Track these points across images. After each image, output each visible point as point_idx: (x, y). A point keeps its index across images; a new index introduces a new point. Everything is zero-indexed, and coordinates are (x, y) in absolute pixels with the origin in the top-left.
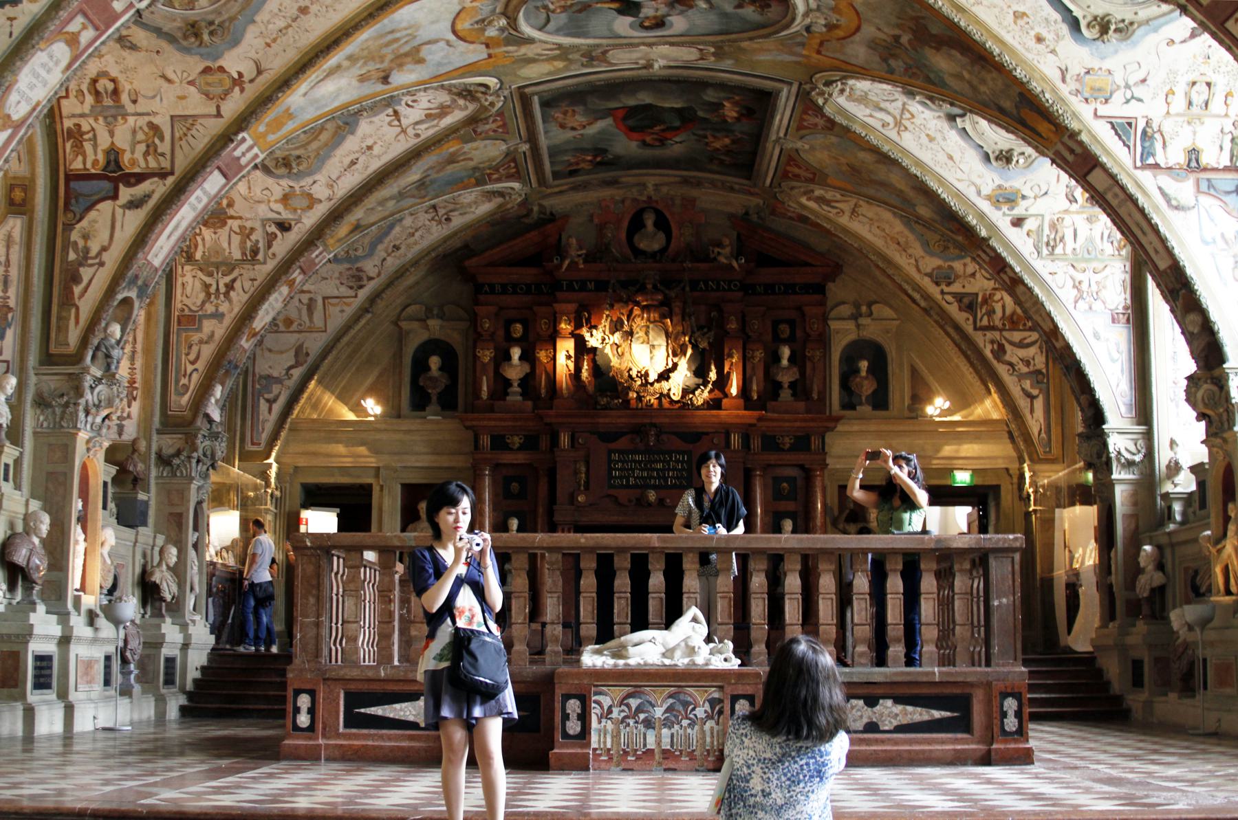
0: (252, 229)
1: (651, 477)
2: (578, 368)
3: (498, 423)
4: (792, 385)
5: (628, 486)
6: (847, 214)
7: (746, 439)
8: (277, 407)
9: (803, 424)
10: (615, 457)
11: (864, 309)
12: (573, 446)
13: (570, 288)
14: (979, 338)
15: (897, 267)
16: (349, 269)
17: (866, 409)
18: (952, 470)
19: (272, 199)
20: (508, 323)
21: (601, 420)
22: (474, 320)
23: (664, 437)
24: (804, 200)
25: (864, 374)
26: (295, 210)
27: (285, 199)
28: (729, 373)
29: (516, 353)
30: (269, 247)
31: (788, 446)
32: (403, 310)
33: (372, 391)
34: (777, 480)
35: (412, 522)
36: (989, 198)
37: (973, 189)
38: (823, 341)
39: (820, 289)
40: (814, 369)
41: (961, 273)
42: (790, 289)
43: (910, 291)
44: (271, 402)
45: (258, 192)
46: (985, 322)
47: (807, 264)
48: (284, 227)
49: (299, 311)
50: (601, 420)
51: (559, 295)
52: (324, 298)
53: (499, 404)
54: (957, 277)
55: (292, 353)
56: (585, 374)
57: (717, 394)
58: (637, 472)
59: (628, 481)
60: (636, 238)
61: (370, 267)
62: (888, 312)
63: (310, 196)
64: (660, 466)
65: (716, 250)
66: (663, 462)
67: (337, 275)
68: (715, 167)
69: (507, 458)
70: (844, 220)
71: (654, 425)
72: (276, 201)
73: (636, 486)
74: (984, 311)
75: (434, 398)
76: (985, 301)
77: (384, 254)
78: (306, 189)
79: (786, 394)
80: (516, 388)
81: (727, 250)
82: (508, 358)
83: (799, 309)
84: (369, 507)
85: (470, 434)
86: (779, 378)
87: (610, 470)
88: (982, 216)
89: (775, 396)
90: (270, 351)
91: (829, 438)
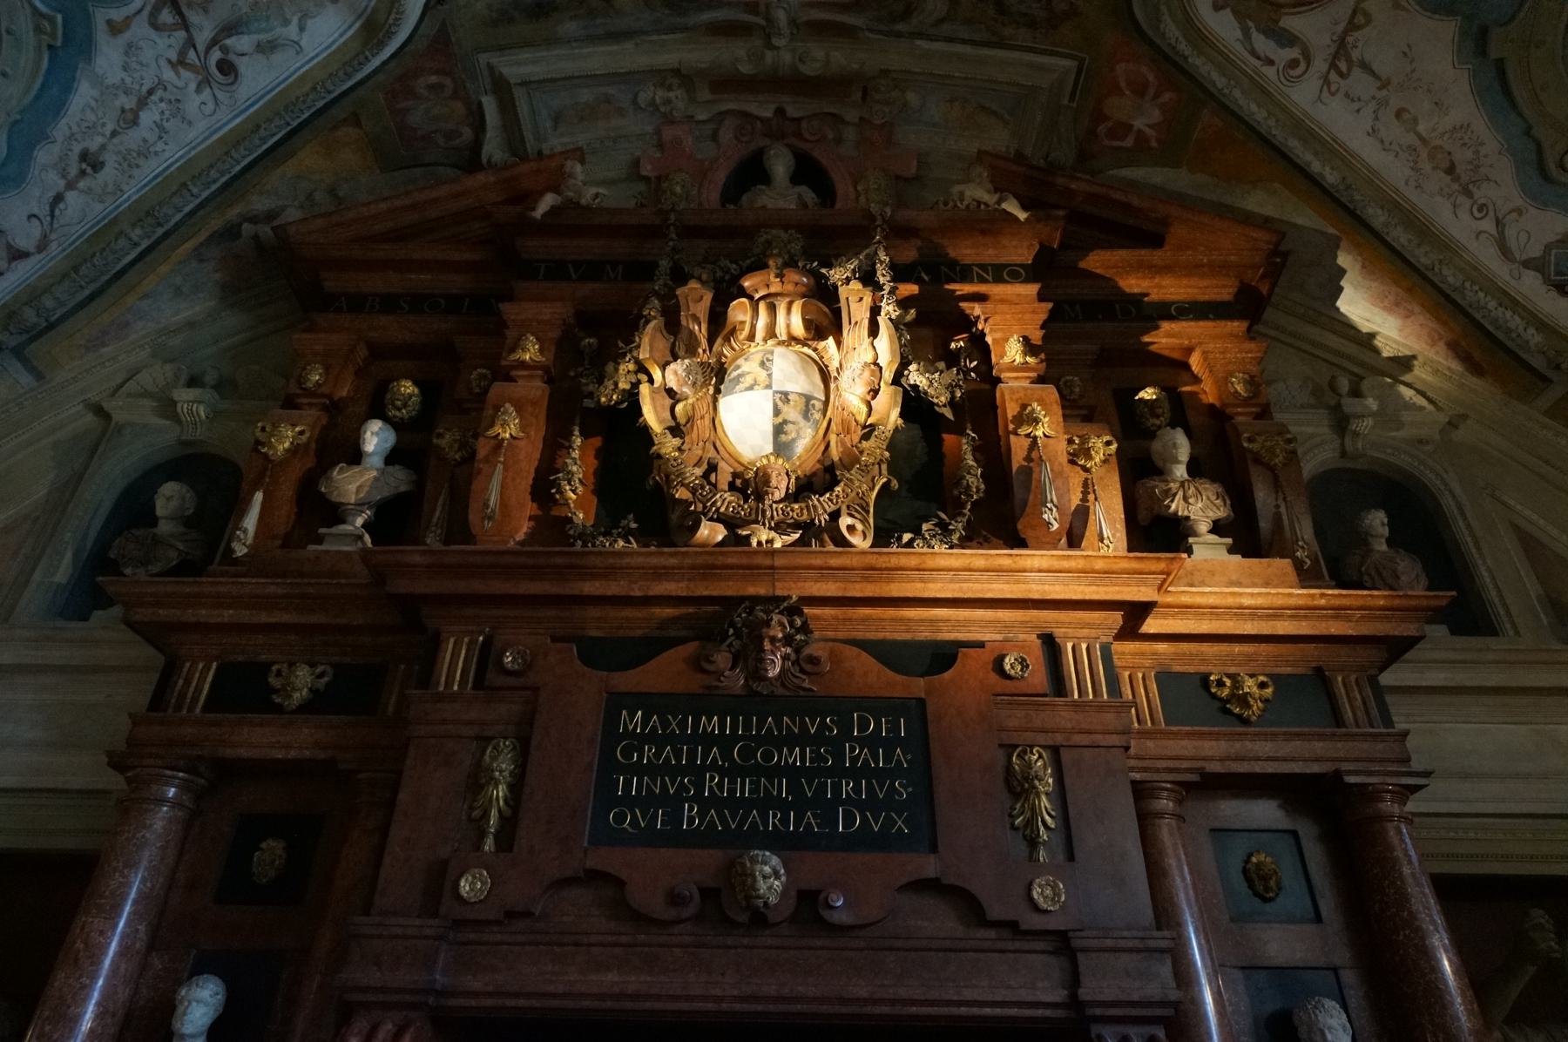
1: (766, 803)
5: (674, 837)
6: (1320, 65)
12: (479, 684)
13: (557, 271)
28: (1027, 472)
29: (375, 438)
58: (711, 781)
59: (674, 817)
64: (795, 757)
66: (818, 740)
69: (256, 740)
70: (1303, 95)
73: (704, 838)
77: (55, 182)
82: (355, 456)
87: (608, 767)
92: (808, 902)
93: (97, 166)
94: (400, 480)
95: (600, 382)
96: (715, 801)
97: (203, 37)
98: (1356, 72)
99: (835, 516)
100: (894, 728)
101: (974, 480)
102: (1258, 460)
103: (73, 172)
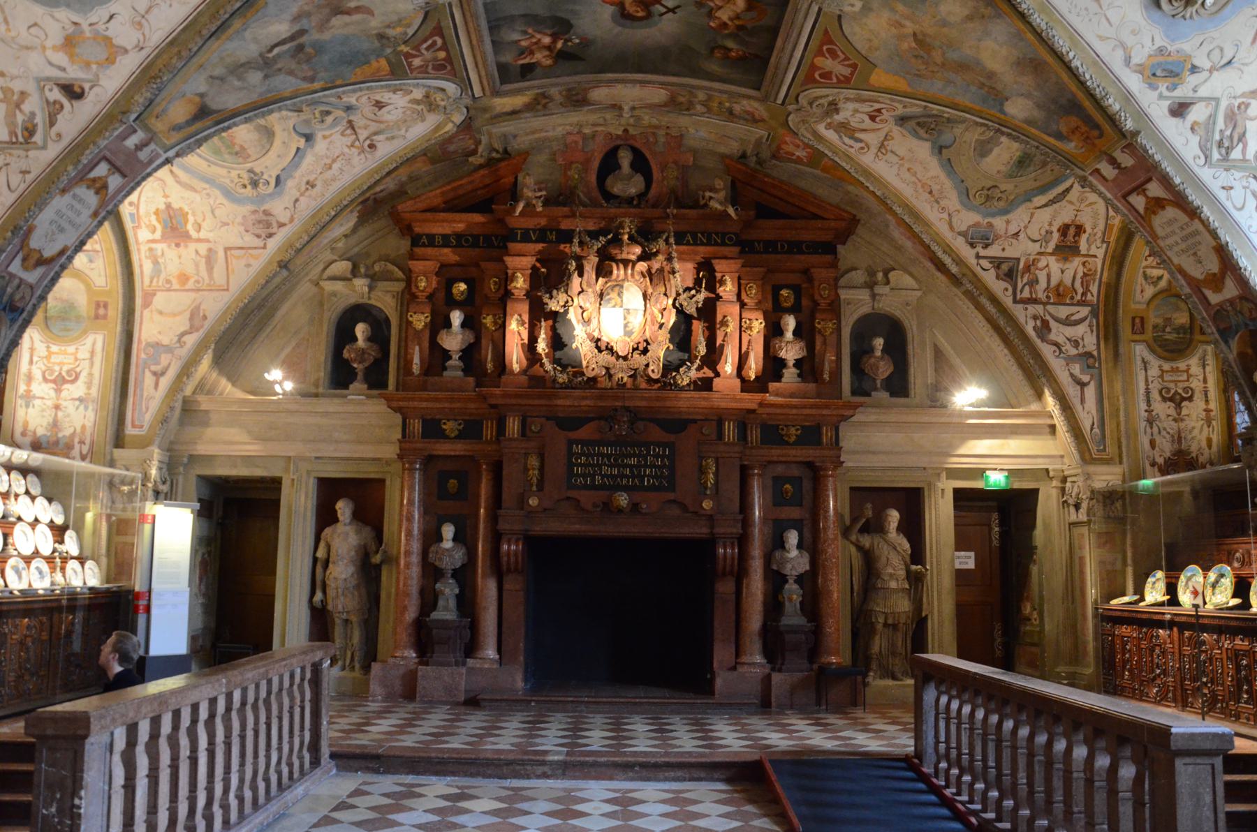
0: (23, 94)
1: (623, 476)
2: (533, 339)
3: (430, 405)
4: (798, 363)
5: (593, 487)
6: (874, 150)
7: (743, 428)
8: (165, 382)
9: (813, 411)
10: (577, 449)
11: (880, 275)
13: (526, 238)
14: (1019, 312)
15: (926, 224)
16: (255, 212)
17: (883, 395)
18: (984, 471)
19: (49, 43)
20: (450, 283)
21: (559, 402)
22: (409, 279)
23: (641, 425)
24: (821, 128)
25: (878, 353)
26: (88, 65)
27: (70, 43)
28: (722, 346)
29: (456, 317)
30: (52, 123)
31: (793, 439)
32: (325, 268)
33: (292, 367)
34: (778, 481)
35: (329, 525)
36: (1140, 69)
37: (1120, 53)
38: (835, 309)
39: (829, 249)
40: (825, 343)
41: (1002, 232)
42: (795, 247)
43: (940, 254)
44: (157, 375)
45: (24, 33)
46: (1026, 294)
47: (816, 217)
48: (73, 92)
49: (197, 265)
50: (559, 402)
51: (514, 247)
52: (226, 249)
53: (432, 380)
54: (997, 237)
55: (187, 315)
56: (542, 346)
57: (708, 373)
58: (604, 469)
59: (593, 480)
60: (609, 181)
61: (279, 208)
62: (908, 281)
63: (108, 40)
65: (708, 194)
66: (639, 456)
67: (239, 219)
68: (714, 67)
69: (443, 448)
70: (867, 159)
71: (628, 409)
72: (54, 48)
73: (602, 487)
74: (1025, 280)
75: (360, 376)
76: (1028, 268)
77: (296, 194)
78: (101, 27)
79: (790, 374)
80: (455, 361)
81: (722, 195)
82: (448, 325)
83: (806, 271)
84: (276, 504)
85: (398, 418)
86: (783, 354)
87: (570, 466)
88: (1128, 97)
89: (778, 377)
90: (161, 313)
91: (843, 428)
92: (635, 507)
93: (313, 186)
94: (471, 338)
95: (551, 298)
96: (605, 476)
97: (362, 138)
98: (889, 154)
99: (647, 365)
100: (664, 451)
101: (702, 350)
102: (820, 332)
103: (303, 188)
